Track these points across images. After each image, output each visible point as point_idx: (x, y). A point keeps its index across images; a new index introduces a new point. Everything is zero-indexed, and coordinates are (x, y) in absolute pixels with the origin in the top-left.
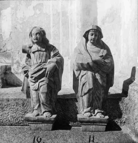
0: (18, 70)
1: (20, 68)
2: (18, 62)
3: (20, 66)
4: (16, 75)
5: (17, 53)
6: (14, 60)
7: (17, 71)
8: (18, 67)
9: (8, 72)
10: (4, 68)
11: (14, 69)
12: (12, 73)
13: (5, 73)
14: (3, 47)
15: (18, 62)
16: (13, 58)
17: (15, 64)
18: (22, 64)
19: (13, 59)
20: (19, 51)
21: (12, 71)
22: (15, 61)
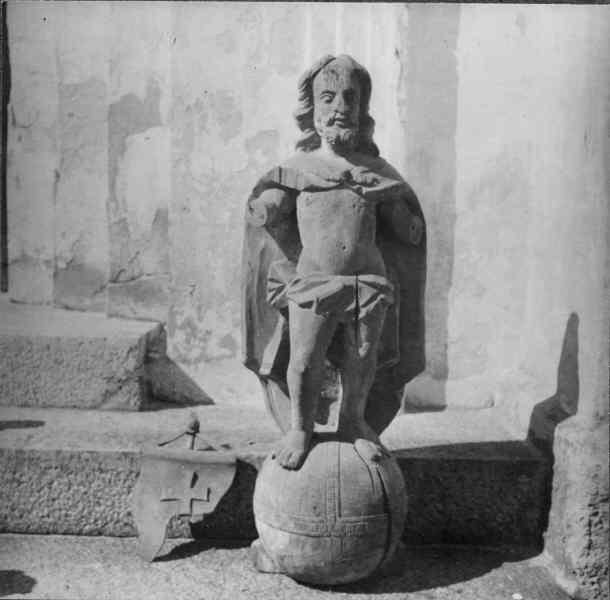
0: (190, 350)
1: (197, 342)
2: (189, 323)
3: (195, 337)
4: (183, 367)
5: (187, 293)
6: (178, 317)
7: (183, 351)
8: (188, 341)
9: (157, 356)
10: (144, 342)
11: (175, 348)
12: (168, 361)
13: (148, 360)
14: (131, 262)
15: (189, 323)
16: (175, 309)
17: (181, 328)
18: (204, 332)
19: (177, 312)
20: (194, 286)
21: (170, 352)
22: (180, 320)
